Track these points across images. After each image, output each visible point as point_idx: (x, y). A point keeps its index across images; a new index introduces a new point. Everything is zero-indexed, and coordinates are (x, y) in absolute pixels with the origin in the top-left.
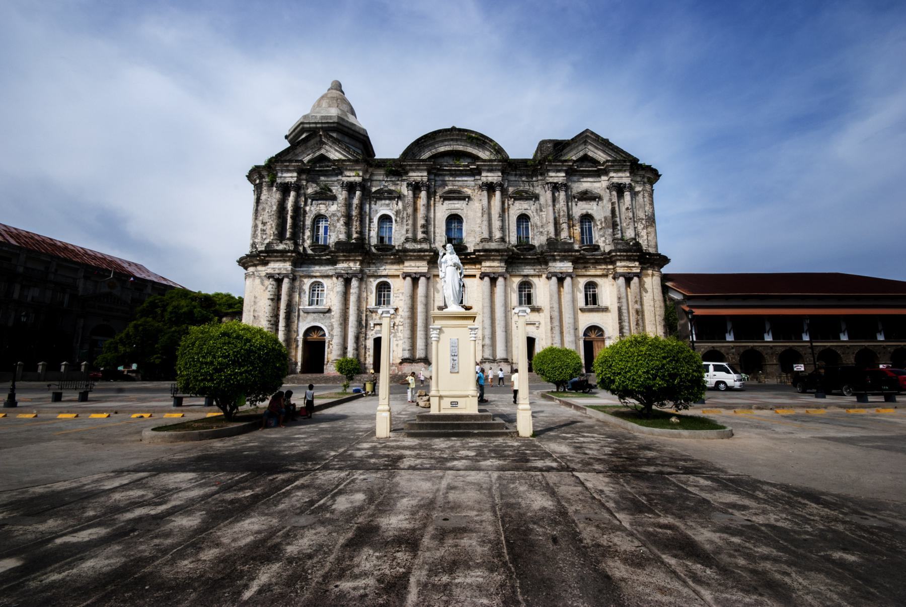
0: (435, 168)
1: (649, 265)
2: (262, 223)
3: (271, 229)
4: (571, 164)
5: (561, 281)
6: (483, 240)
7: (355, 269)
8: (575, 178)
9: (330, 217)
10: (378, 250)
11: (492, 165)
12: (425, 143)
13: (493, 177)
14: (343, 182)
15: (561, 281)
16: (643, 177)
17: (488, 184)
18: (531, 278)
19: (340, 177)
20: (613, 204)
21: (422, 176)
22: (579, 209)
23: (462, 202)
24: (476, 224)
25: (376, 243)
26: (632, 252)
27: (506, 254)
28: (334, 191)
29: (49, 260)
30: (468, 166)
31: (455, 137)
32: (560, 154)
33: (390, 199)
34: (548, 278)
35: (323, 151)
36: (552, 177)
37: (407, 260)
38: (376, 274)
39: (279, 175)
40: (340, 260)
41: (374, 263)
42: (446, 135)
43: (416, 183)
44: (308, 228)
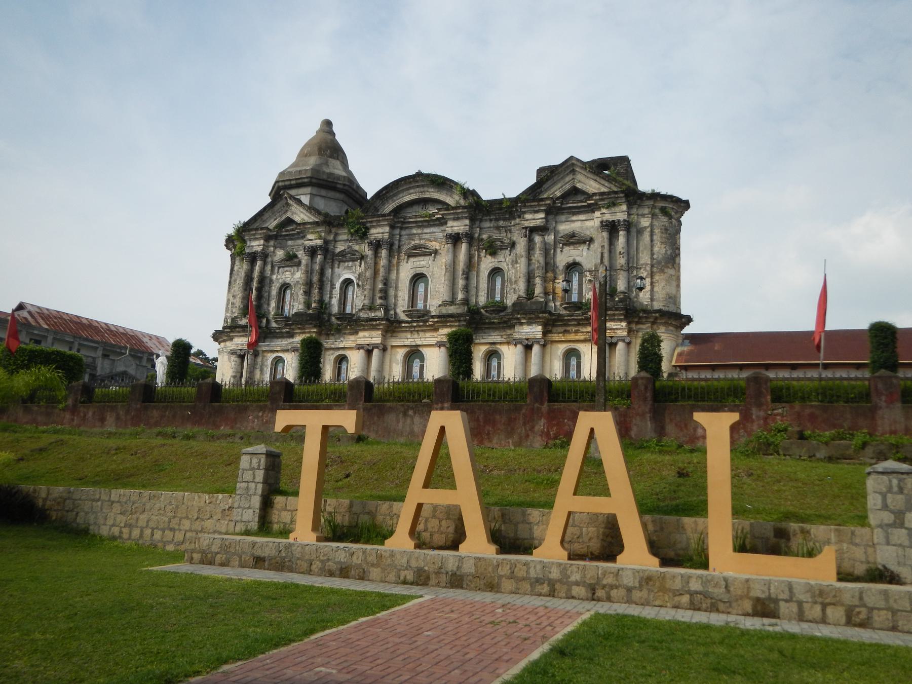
0: (398, 222)
1: (650, 325)
2: (233, 296)
3: (238, 302)
4: (548, 202)
5: (528, 348)
6: (444, 304)
8: (563, 218)
9: (295, 285)
10: (338, 319)
11: (457, 213)
12: (387, 194)
13: (458, 226)
14: (305, 247)
15: (528, 348)
16: (654, 207)
17: (453, 236)
18: (498, 346)
20: (603, 247)
21: (383, 233)
22: (564, 257)
23: (427, 258)
24: (441, 284)
25: (336, 312)
26: (613, 310)
27: (462, 319)
28: (299, 256)
29: (72, 340)
30: (433, 215)
31: (420, 184)
32: (539, 190)
33: (353, 260)
34: (516, 345)
36: (527, 220)
37: (361, 330)
38: (333, 346)
39: (248, 243)
40: (297, 333)
41: (333, 335)
42: (410, 183)
43: (377, 241)
44: (273, 299)
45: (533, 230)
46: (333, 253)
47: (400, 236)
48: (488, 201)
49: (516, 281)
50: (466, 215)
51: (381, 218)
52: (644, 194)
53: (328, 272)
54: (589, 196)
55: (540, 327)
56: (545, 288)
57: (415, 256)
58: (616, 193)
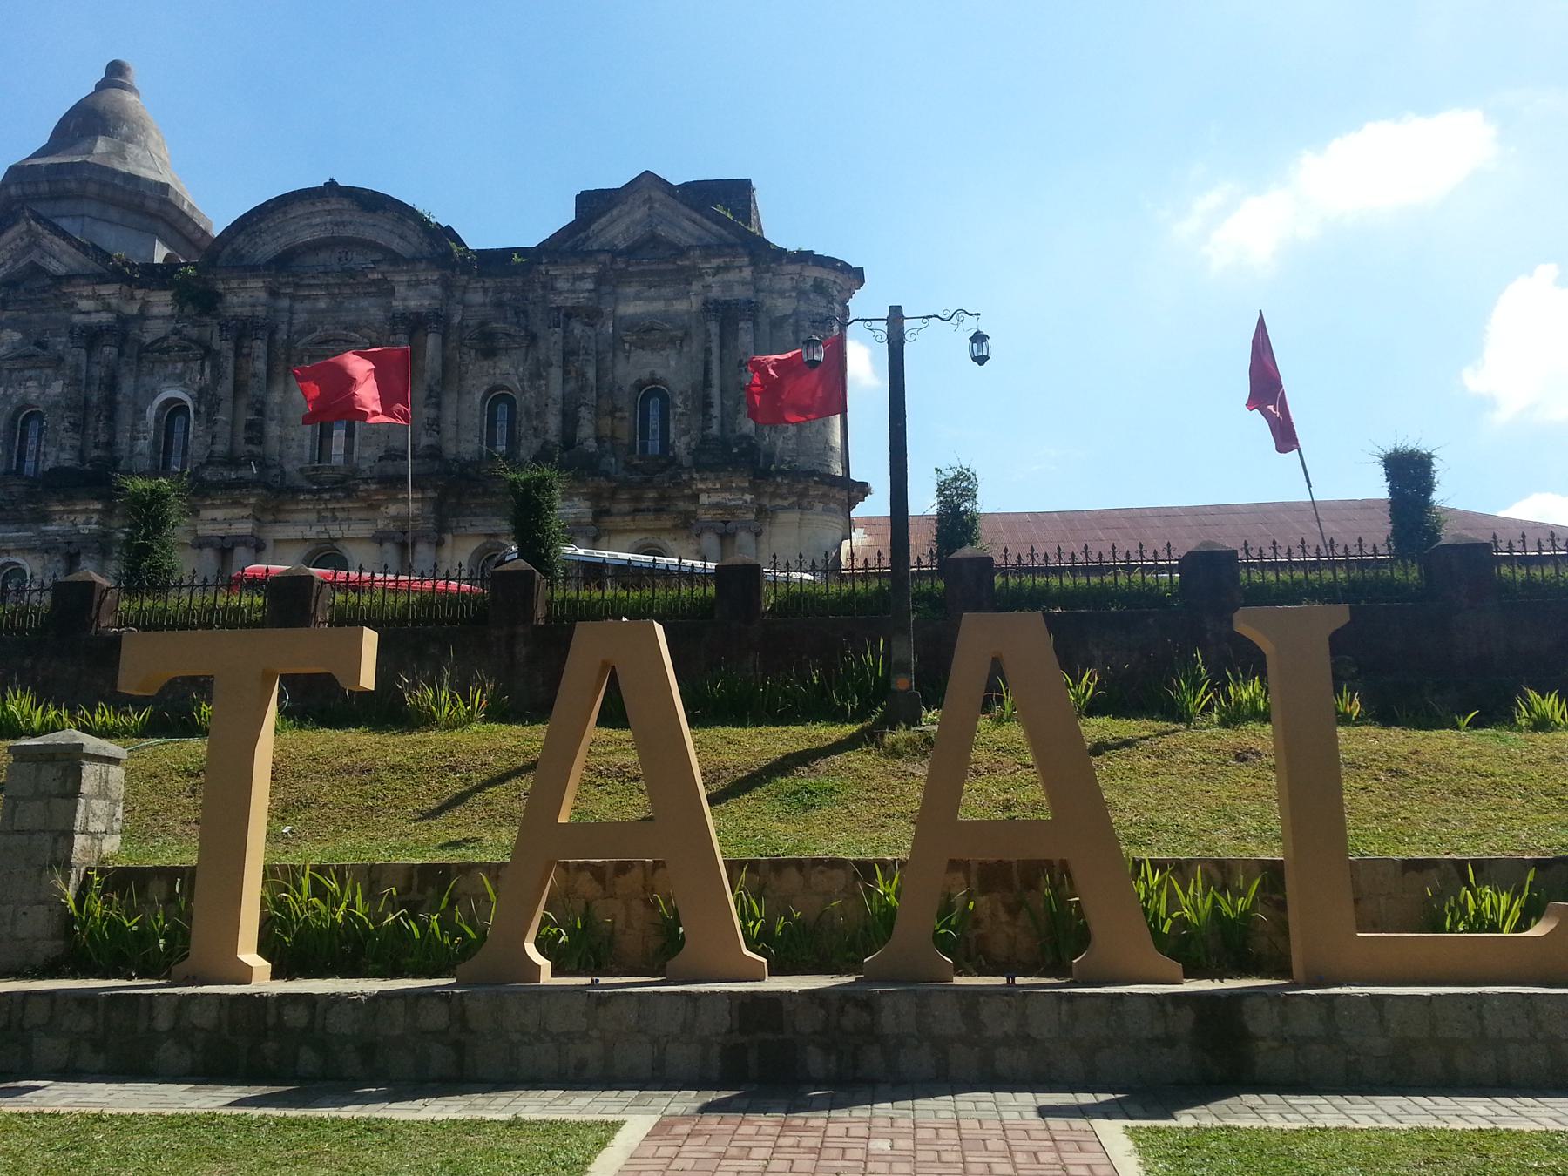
1: (796, 499)
7: (87, 532)
8: (630, 290)
21: (253, 305)
30: (363, 272)
31: (333, 207)
32: (582, 235)
33: (185, 361)
36: (561, 293)
37: (206, 507)
45: (570, 314)
47: (292, 313)
48: (480, 252)
49: (537, 413)
50: (435, 278)
51: (248, 274)
52: (781, 253)
53: (127, 385)
54: (681, 252)
55: (588, 503)
56: (597, 429)
58: (732, 246)
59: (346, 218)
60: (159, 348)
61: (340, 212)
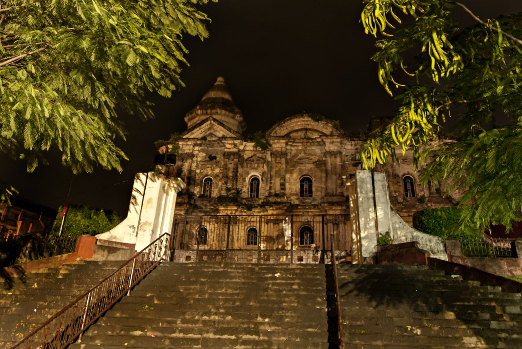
19: (223, 148)
21: (282, 148)
35: (212, 131)
46: (244, 158)
53: (240, 170)
57: (302, 164)
59: (309, 123)
60: (249, 160)
61: (307, 121)
